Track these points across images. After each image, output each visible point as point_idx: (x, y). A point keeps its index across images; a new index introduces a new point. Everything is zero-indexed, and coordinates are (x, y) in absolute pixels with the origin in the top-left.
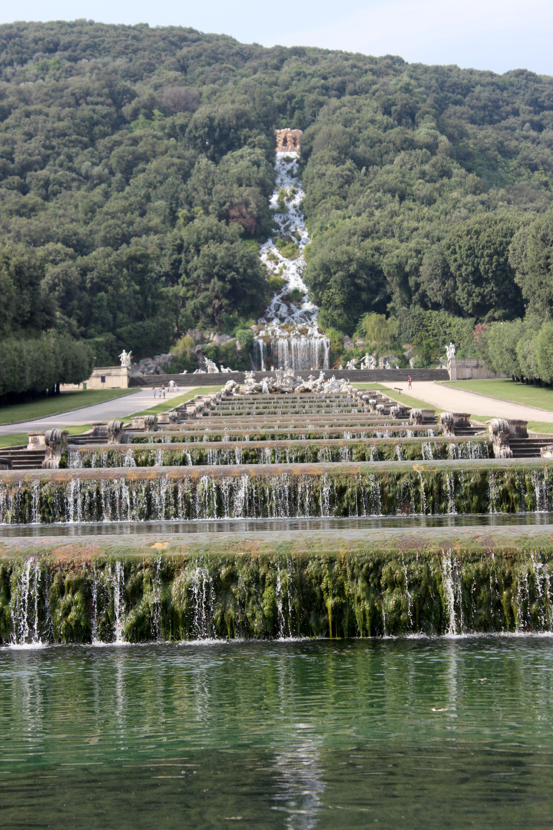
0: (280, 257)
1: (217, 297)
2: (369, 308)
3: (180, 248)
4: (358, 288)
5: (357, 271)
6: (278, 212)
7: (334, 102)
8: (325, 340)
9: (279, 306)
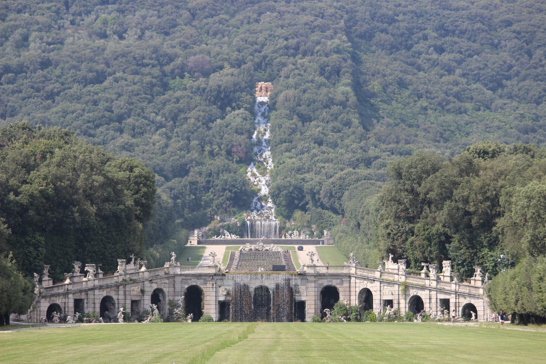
0: (257, 174)
1: (228, 199)
4: (294, 198)
5: (293, 190)
6: (257, 145)
8: (278, 222)
9: (257, 203)
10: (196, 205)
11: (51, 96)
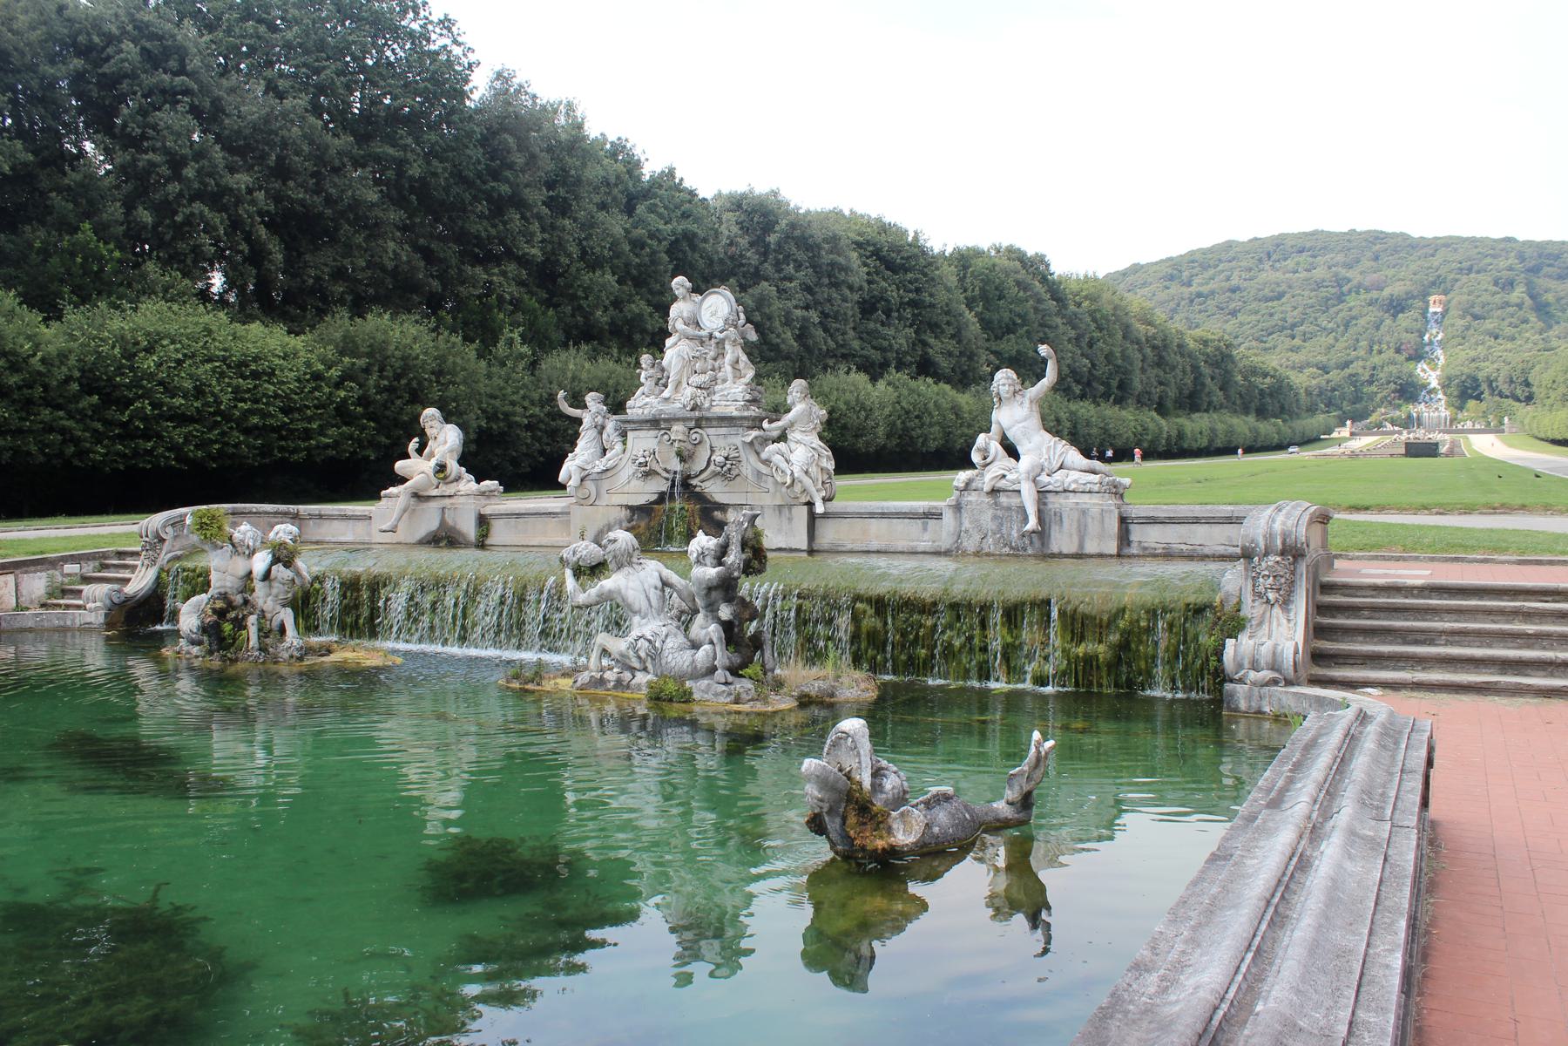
2: (1471, 397)
3: (1374, 368)
7: (1464, 279)
10: (1357, 399)
11: (1234, 313)
